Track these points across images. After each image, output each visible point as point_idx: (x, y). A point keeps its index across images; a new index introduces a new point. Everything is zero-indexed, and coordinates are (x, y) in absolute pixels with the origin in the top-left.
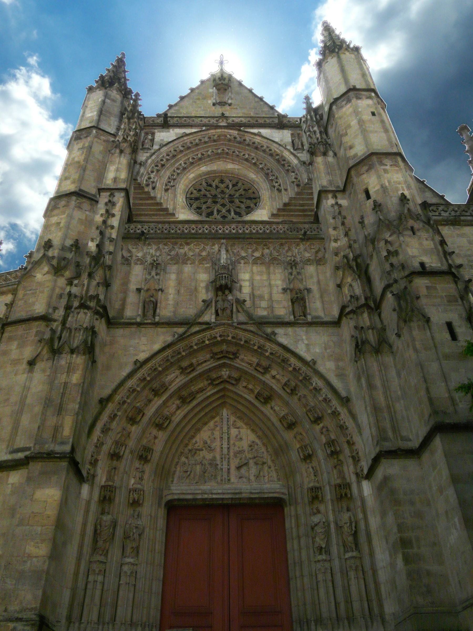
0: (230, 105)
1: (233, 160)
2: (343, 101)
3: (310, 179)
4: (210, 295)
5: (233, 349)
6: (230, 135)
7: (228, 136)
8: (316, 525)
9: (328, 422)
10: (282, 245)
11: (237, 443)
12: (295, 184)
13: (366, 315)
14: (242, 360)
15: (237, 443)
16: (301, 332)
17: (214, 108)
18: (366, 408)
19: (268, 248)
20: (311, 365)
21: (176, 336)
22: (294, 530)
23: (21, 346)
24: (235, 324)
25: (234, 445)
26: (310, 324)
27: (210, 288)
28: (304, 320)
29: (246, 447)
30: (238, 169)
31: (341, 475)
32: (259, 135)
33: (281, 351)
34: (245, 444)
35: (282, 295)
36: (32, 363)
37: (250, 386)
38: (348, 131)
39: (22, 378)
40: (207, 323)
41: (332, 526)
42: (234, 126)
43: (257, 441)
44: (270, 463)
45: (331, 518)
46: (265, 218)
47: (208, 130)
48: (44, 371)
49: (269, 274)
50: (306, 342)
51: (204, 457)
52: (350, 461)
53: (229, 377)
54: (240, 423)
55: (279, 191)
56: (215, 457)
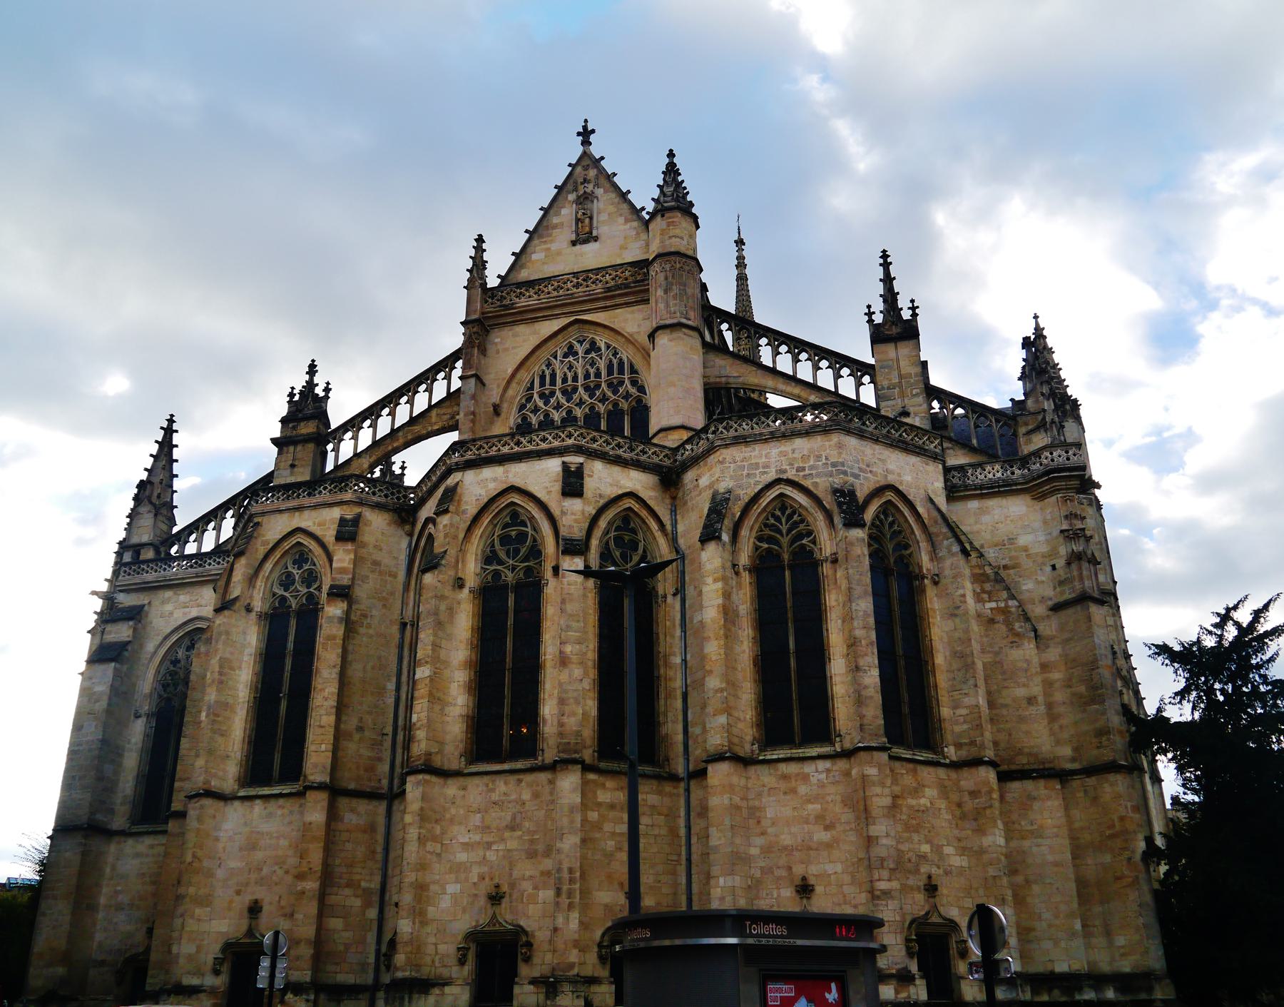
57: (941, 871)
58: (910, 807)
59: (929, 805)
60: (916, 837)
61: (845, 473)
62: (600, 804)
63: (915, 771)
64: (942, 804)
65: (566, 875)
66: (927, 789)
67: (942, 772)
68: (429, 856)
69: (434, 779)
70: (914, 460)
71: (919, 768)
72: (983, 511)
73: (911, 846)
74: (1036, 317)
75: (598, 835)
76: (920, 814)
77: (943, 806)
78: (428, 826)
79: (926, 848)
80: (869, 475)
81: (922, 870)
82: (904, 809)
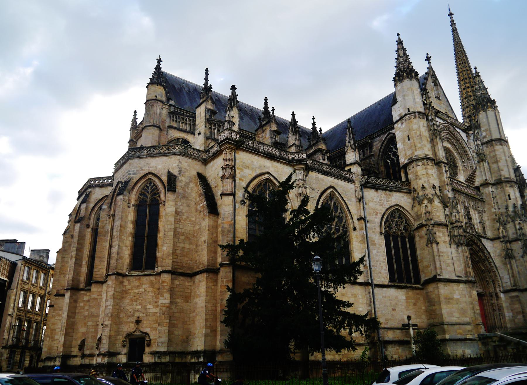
0: (440, 100)
3: (476, 168)
20: (489, 253)
23: (444, 236)
27: (467, 217)
32: (459, 133)
33: (483, 247)
39: (449, 249)
48: (455, 248)
57: (145, 315)
58: (134, 293)
59: (144, 291)
60: (135, 303)
61: (130, 174)
62: (84, 301)
63: (140, 279)
64: (150, 290)
65: (63, 325)
66: (144, 285)
67: (152, 278)
68: (56, 321)
69: (60, 298)
70: (165, 158)
71: (142, 277)
72: (213, 165)
73: (132, 307)
75: (82, 311)
76: (139, 295)
77: (150, 290)
78: (57, 312)
79: (139, 307)
80: (141, 171)
81: (135, 315)
82: (132, 294)
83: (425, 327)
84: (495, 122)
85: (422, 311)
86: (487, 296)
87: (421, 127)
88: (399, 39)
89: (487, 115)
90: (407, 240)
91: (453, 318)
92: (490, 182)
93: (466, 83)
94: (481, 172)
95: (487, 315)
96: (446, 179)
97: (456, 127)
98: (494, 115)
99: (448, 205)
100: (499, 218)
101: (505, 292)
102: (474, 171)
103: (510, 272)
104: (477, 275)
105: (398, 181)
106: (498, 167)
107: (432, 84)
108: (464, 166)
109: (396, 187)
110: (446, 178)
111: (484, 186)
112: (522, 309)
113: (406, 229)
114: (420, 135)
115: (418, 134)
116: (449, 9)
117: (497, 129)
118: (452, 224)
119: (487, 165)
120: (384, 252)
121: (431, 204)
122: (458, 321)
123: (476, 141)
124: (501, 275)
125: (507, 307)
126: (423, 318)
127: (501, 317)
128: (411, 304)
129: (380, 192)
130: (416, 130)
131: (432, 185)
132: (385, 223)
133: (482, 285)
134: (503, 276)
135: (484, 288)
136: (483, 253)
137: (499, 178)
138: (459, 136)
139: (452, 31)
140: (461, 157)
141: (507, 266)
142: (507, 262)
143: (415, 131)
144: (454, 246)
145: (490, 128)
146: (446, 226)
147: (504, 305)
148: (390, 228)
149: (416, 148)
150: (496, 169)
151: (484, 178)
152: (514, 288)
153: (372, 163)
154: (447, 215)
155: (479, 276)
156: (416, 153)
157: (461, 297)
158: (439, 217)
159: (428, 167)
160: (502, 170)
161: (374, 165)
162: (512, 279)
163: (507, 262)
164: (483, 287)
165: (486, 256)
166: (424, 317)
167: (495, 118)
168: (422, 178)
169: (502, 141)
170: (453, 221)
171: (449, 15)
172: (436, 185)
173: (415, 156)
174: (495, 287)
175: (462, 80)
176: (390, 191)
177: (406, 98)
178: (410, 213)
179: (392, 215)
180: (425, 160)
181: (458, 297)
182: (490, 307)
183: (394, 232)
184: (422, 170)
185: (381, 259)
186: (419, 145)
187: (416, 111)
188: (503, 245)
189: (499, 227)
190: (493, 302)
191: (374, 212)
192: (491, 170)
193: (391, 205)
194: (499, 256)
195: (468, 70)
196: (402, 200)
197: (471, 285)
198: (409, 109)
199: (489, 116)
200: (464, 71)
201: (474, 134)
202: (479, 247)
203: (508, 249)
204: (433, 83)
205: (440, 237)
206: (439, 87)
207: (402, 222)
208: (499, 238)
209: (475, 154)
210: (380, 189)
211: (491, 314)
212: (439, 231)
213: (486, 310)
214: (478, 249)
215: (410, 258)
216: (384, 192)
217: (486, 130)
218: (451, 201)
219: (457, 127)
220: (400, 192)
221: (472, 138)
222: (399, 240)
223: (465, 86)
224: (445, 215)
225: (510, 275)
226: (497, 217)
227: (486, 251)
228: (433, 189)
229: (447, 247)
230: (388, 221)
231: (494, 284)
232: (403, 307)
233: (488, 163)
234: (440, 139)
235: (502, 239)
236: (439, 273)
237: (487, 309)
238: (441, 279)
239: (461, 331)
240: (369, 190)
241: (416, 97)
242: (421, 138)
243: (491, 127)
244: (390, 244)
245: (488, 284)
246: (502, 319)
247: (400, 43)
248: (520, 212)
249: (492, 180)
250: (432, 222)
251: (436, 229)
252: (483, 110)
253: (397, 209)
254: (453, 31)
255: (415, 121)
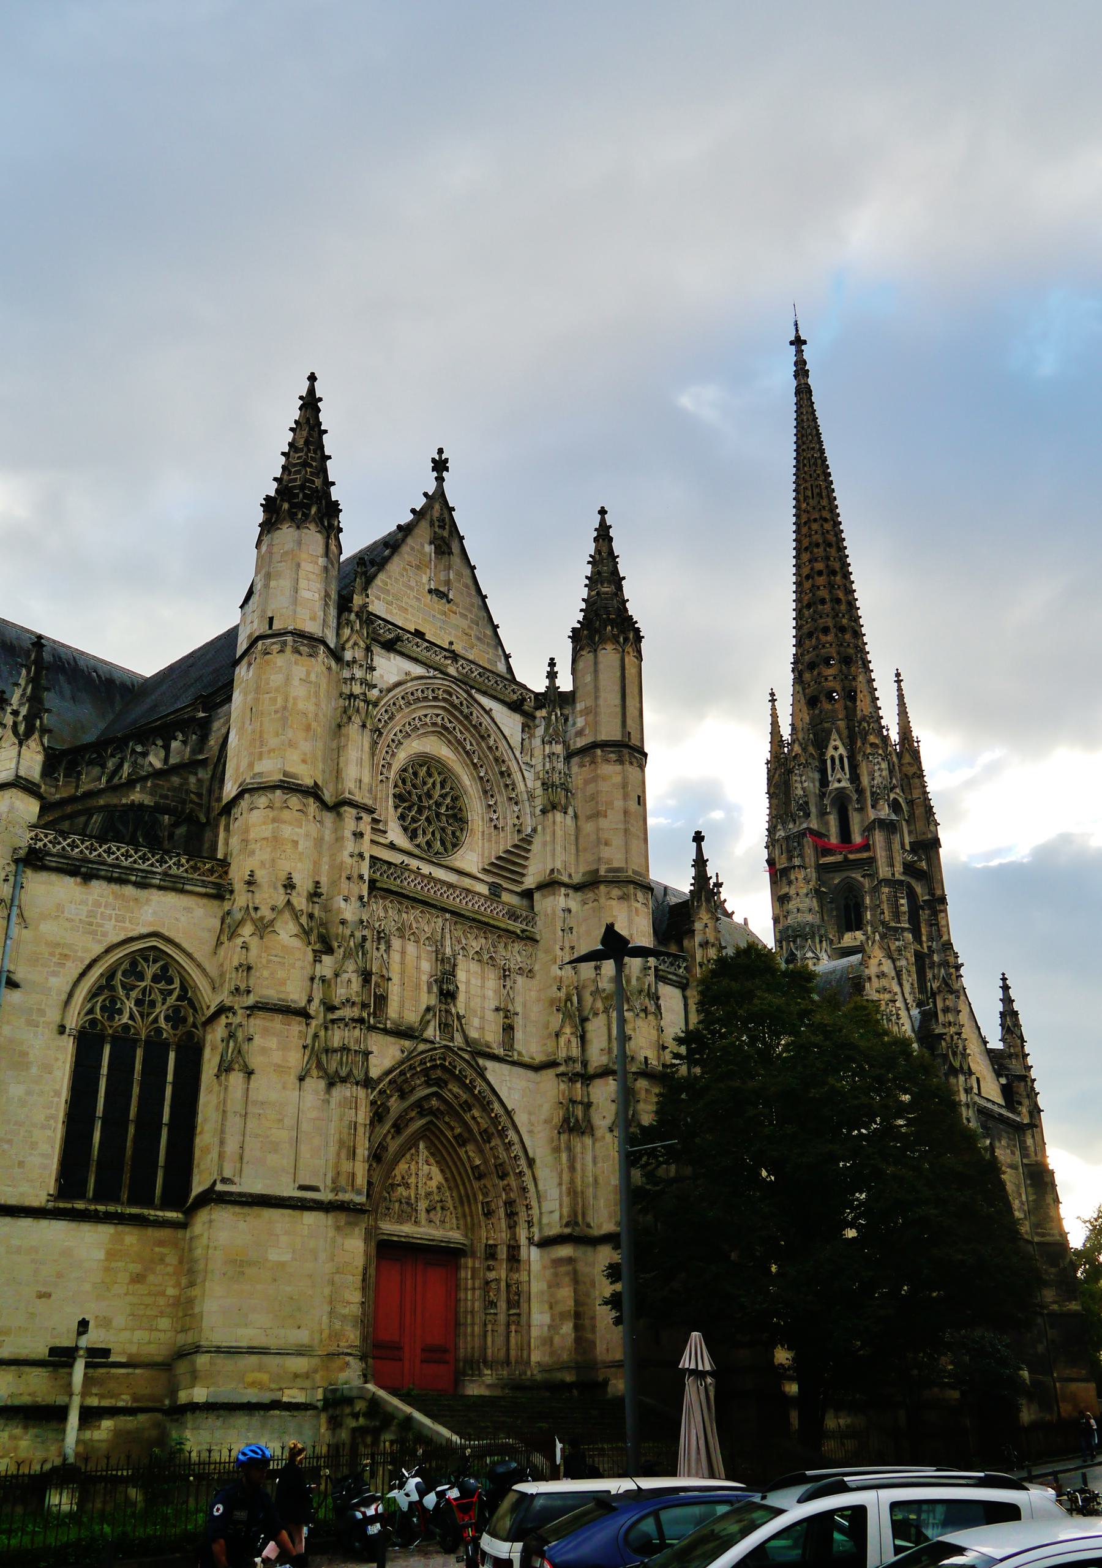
0: (449, 601)
1: (450, 742)
2: (612, 752)
3: (534, 830)
4: (433, 1001)
5: (446, 1077)
6: (457, 698)
7: (454, 697)
8: (491, 1281)
9: (512, 1181)
10: (499, 936)
11: (428, 1182)
12: (516, 828)
13: (579, 1085)
14: (450, 1091)
15: (428, 1182)
16: (505, 1068)
17: (429, 597)
18: (560, 1184)
19: (486, 938)
20: (509, 1113)
21: (406, 1054)
22: (470, 1282)
23: (284, 1047)
24: (456, 1049)
25: (425, 1183)
26: (514, 1063)
27: (435, 989)
28: (510, 1057)
29: (435, 1190)
30: (453, 760)
31: (514, 1237)
32: (488, 712)
33: (488, 1092)
34: (433, 1184)
35: (492, 1013)
36: (301, 1079)
37: (452, 1123)
38: (609, 812)
40: (432, 1042)
41: (503, 1285)
42: (465, 683)
43: (443, 1182)
44: (452, 1208)
45: (503, 1276)
46: (474, 871)
47: (435, 677)
49: (483, 978)
50: (509, 1085)
51: (401, 1194)
52: (526, 1225)
53: (438, 1109)
54: (432, 1160)
55: (495, 827)
56: (410, 1196)
74: (312, 378)
83: (159, 1359)
84: (617, 688)
85: (162, 1301)
86: (473, 1255)
87: (296, 682)
88: (311, 391)
89: (596, 663)
90: (172, 1055)
91: (241, 1332)
92: (565, 879)
93: (816, 560)
94: (545, 844)
95: (462, 1321)
96: (349, 860)
97: (479, 691)
98: (617, 664)
99: (336, 944)
100: (569, 999)
101: (546, 1243)
102: (528, 840)
103: (566, 1177)
104: (452, 1184)
105: (178, 855)
106: (598, 830)
107: (429, 549)
108: (491, 820)
109: (165, 874)
110: (352, 856)
111: (545, 892)
112: (577, 1303)
113: (175, 1018)
114: (285, 708)
115: (280, 702)
116: (796, 324)
117: (619, 710)
118: (330, 1008)
119: (569, 821)
120: (57, 1094)
121: (261, 938)
122: (260, 1341)
123: (551, 743)
124: (541, 1187)
125: (542, 1293)
126: (160, 1327)
127: (513, 1328)
128: (123, 1277)
129: (98, 888)
130: (277, 690)
131: (283, 875)
132: (93, 995)
133: (464, 1216)
134: (546, 1191)
135: (471, 1229)
136: (486, 1107)
137: (594, 867)
138: (486, 721)
139: (796, 394)
140: (485, 792)
141: (560, 1157)
142: (563, 1146)
143: (271, 695)
144: (315, 1085)
145: (597, 706)
146: (303, 1014)
147: (537, 1286)
148: (112, 1009)
149: (265, 749)
150: (593, 837)
151: (549, 867)
152: (567, 1231)
153: (193, 787)
154: (323, 979)
155: (457, 1186)
156: (257, 769)
157: (294, 1259)
158: (283, 983)
159: (286, 815)
160: (606, 844)
161: (199, 795)
162: (566, 1200)
163: (563, 1146)
164: (466, 1225)
165: (495, 1121)
166: (164, 1323)
167: (618, 674)
168: (257, 852)
169: (625, 751)
170: (336, 1002)
171: (792, 343)
172: (297, 879)
173: (254, 776)
174: (512, 1227)
175: (806, 549)
176: (142, 885)
177: (273, 584)
178: (199, 966)
179: (133, 970)
180: (278, 792)
181: (286, 1257)
182: (477, 1292)
183: (126, 1027)
184: (265, 823)
185: (40, 1117)
186: (273, 742)
187: (290, 628)
188: (562, 1086)
189: (562, 1027)
190: (492, 1275)
191: (52, 954)
192: (581, 840)
193: (130, 935)
194: (546, 1122)
195: (826, 520)
196: (183, 919)
197: (342, 1218)
198: (271, 619)
199: (601, 666)
200: (815, 520)
201: (547, 719)
202: (469, 1088)
203: (573, 1102)
204: (431, 543)
205: (264, 1051)
206: (456, 560)
207: (171, 992)
208: (552, 1064)
209: (538, 783)
210: (98, 877)
211: (473, 1317)
212: (266, 1031)
213: (462, 1303)
214: (464, 1096)
215: (166, 1118)
216: (115, 887)
217: (587, 712)
218: (348, 932)
219: (484, 693)
220: (182, 891)
221: (540, 731)
222: (139, 1053)
223: (812, 569)
224: (312, 979)
225: (564, 1187)
226: (562, 994)
227: (496, 1106)
228: (282, 890)
229: (284, 1088)
230: (112, 988)
231: (511, 1215)
232: (87, 1287)
233: (576, 816)
234: (364, 726)
235: (562, 1069)
236: (227, 1174)
237: (466, 1300)
238: (231, 1194)
239: (265, 1377)
240: (54, 877)
241: (303, 584)
242: (284, 719)
243: (601, 702)
244: (100, 1066)
245: (489, 1214)
246: (513, 1334)
247: (310, 403)
248: (634, 982)
249: (577, 872)
250: (250, 1000)
251: (257, 1024)
252: (589, 645)
253: (154, 948)
254: (798, 392)
255: (279, 660)
